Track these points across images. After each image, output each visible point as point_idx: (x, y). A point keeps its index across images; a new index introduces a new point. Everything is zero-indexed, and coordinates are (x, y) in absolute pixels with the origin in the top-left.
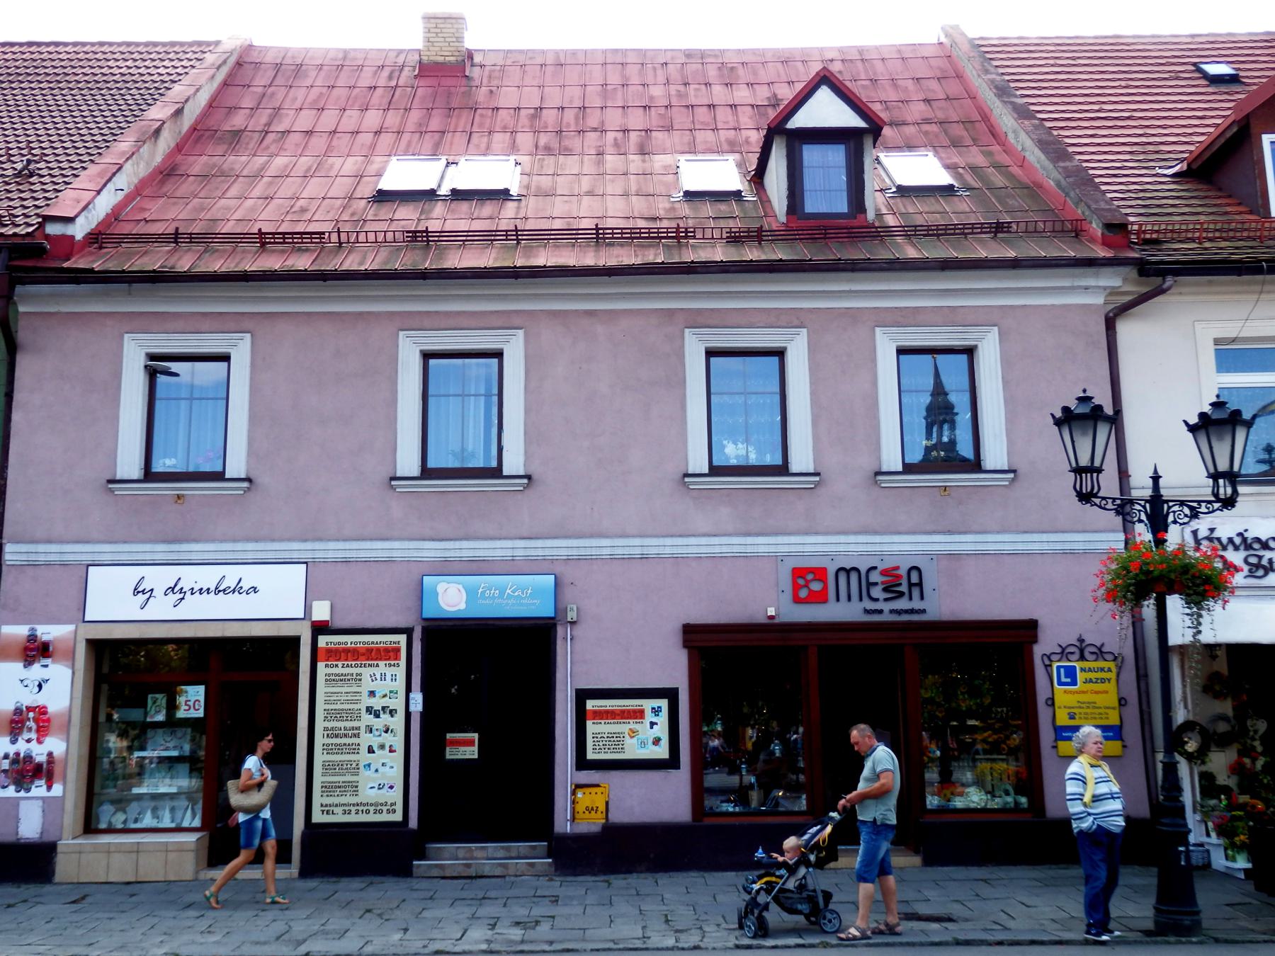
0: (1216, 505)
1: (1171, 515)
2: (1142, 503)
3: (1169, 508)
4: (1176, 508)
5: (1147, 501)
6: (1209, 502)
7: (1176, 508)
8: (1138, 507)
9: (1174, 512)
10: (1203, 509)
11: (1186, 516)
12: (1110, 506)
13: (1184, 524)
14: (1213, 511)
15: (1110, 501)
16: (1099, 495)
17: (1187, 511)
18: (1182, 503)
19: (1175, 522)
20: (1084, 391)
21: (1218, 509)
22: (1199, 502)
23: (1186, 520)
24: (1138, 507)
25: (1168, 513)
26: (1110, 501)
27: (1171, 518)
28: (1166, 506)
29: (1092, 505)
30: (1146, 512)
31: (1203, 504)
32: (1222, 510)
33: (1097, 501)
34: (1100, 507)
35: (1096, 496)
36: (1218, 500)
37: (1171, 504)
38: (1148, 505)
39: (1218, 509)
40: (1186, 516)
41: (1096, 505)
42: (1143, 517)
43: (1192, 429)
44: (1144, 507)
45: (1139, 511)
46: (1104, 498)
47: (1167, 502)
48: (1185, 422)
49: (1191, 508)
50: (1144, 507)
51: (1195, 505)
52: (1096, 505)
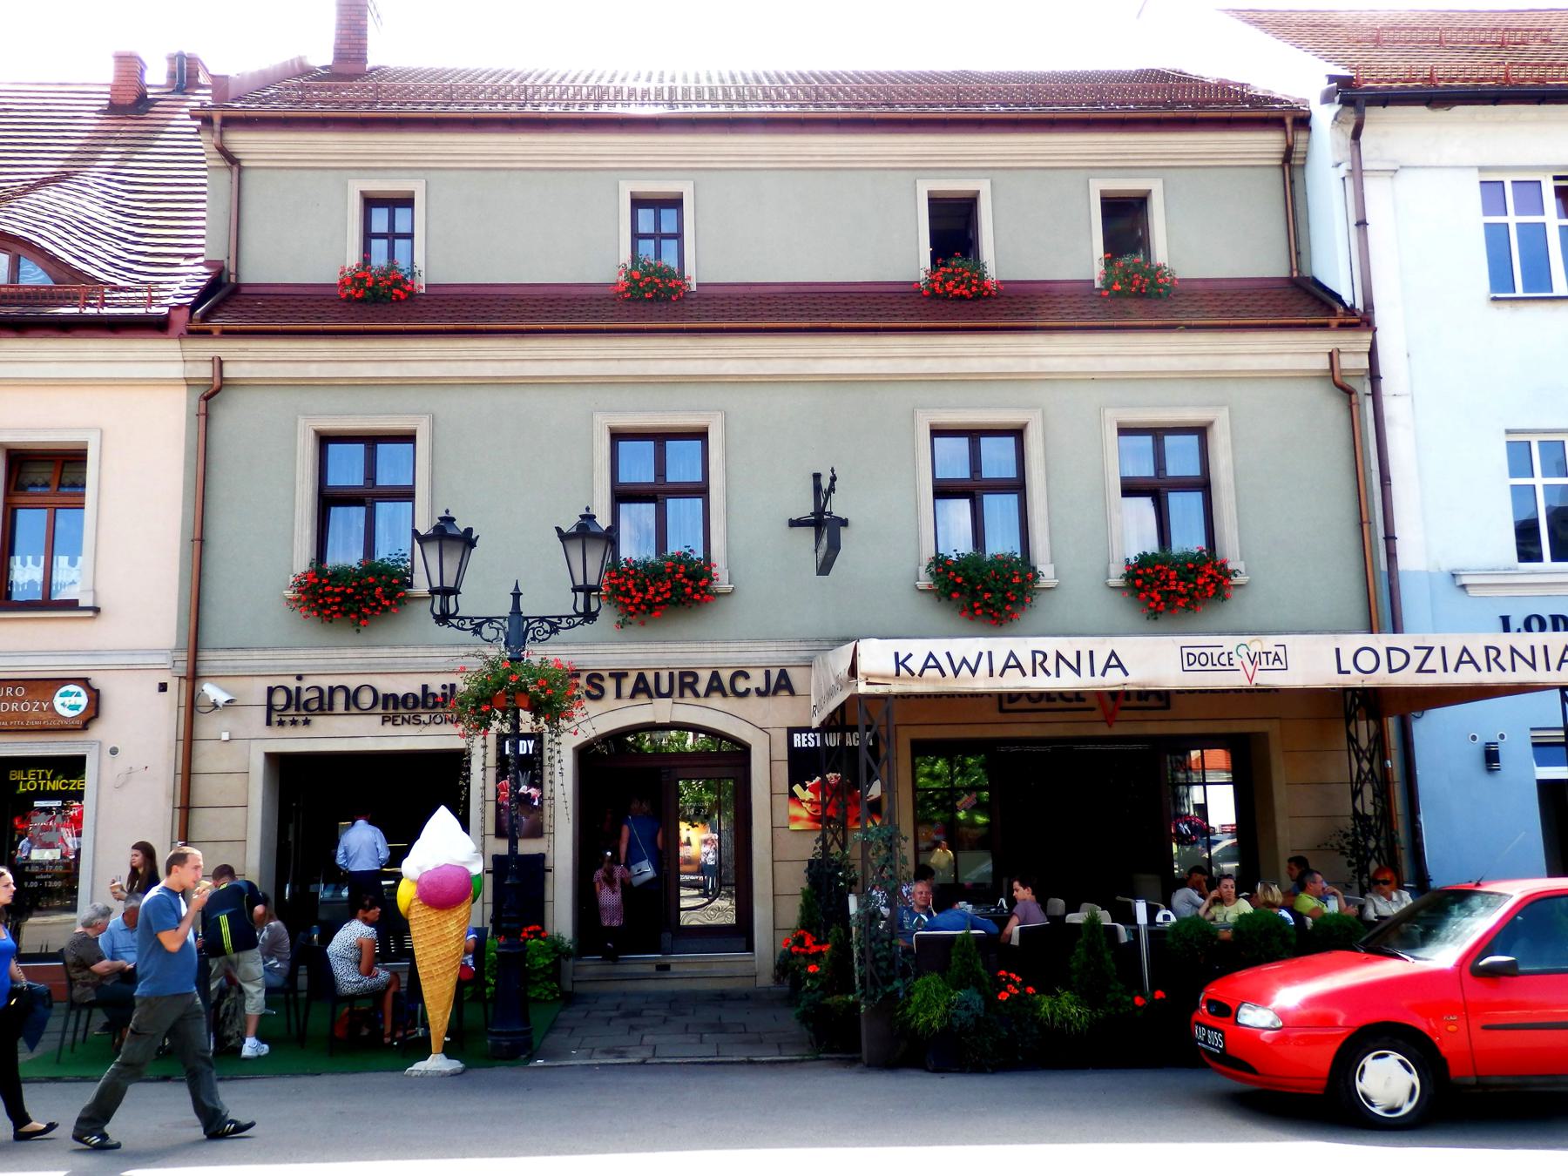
0: (577, 620)
2: (501, 621)
3: (529, 625)
6: (570, 617)
8: (495, 625)
10: (564, 624)
11: (546, 632)
12: (468, 626)
14: (574, 626)
15: (468, 621)
17: (546, 627)
18: (542, 619)
19: (534, 639)
21: (579, 623)
22: (560, 618)
23: (546, 636)
24: (495, 625)
25: (527, 630)
27: (530, 634)
28: (525, 623)
31: (564, 620)
33: (455, 621)
34: (458, 628)
35: (454, 616)
36: (579, 615)
37: (530, 621)
39: (579, 623)
40: (546, 632)
41: (453, 625)
43: (564, 536)
45: (498, 629)
46: (462, 618)
48: (558, 529)
49: (551, 624)
51: (556, 620)
52: (453, 625)
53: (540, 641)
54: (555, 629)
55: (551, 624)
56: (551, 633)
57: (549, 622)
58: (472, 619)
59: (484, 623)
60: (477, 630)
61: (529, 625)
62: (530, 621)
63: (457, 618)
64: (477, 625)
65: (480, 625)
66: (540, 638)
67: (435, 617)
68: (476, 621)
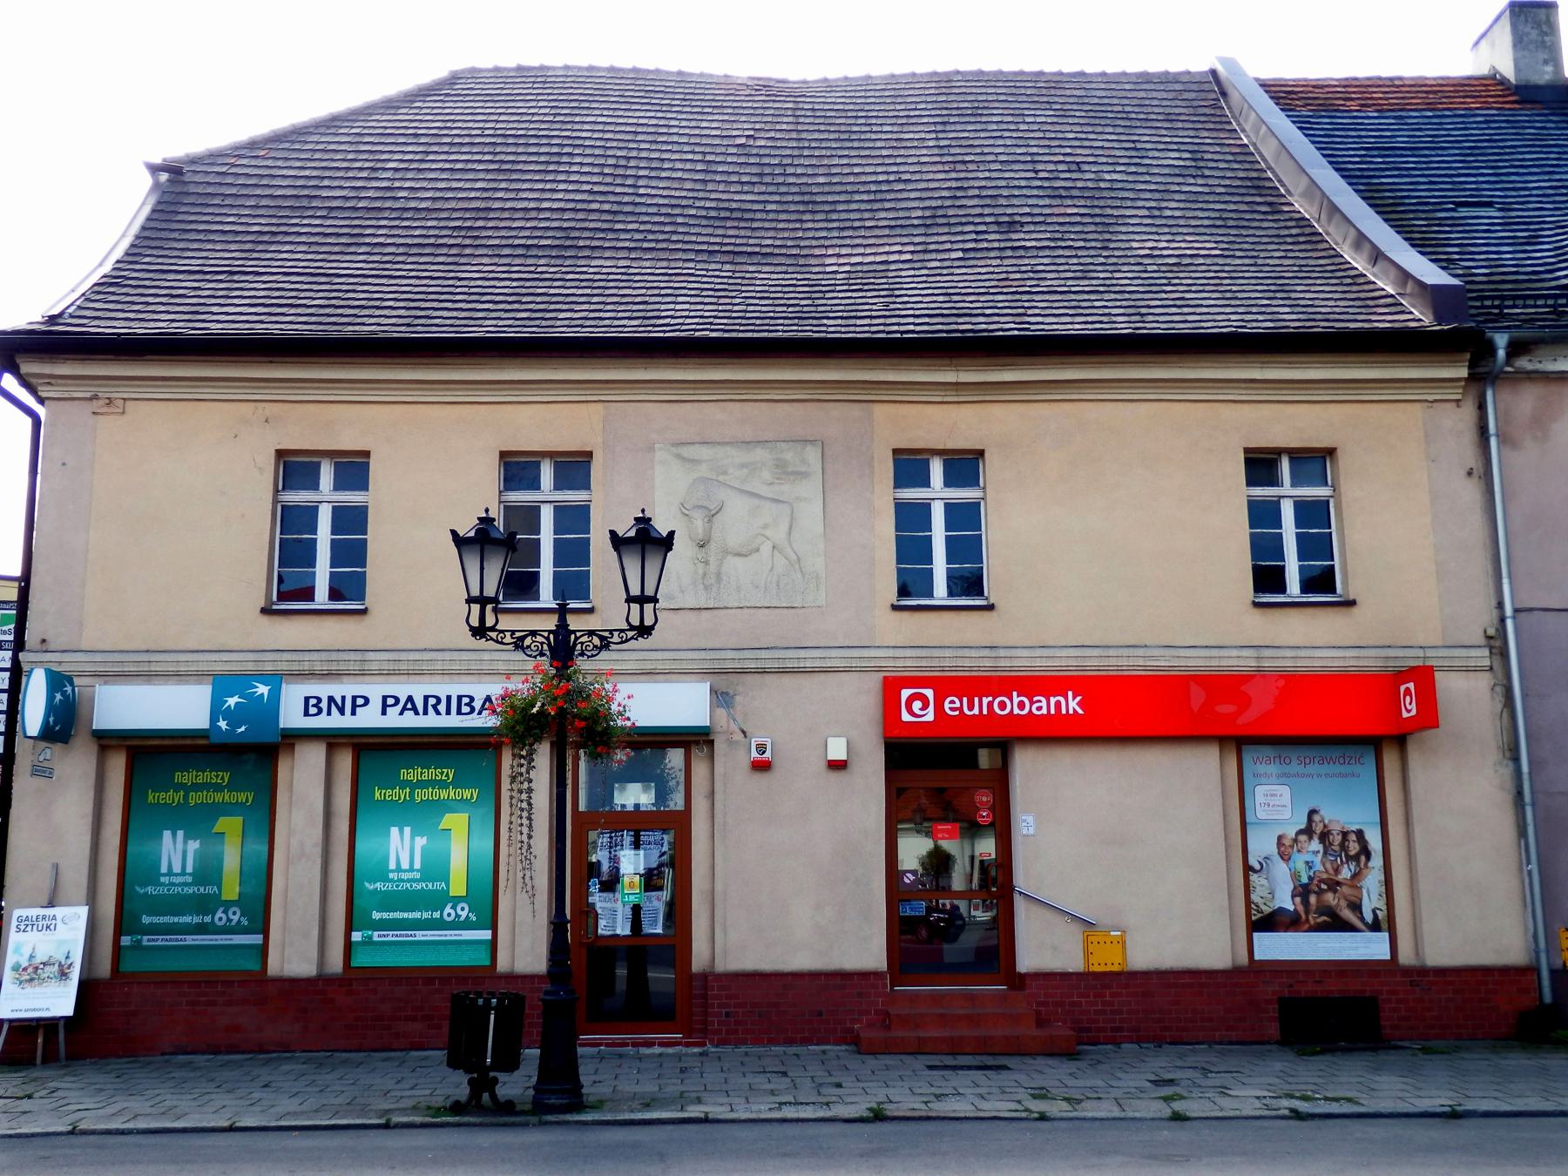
0: (630, 634)
3: (576, 638)
4: (585, 639)
5: (550, 632)
6: (622, 631)
7: (585, 639)
9: (582, 643)
10: (616, 639)
12: (508, 639)
14: (627, 641)
15: (508, 634)
16: (498, 627)
17: (596, 641)
19: (582, 654)
20: (643, 511)
21: (632, 638)
22: (611, 631)
25: (575, 645)
28: (573, 637)
29: (487, 640)
30: (549, 645)
31: (616, 634)
32: (636, 639)
33: (493, 635)
34: (497, 641)
35: (493, 629)
36: (632, 628)
37: (578, 634)
38: (552, 636)
39: (632, 638)
40: (595, 646)
41: (492, 639)
44: (548, 638)
45: (542, 643)
47: (574, 632)
49: (602, 638)
50: (548, 638)
52: (492, 639)
53: (589, 657)
54: (605, 645)
55: (602, 638)
57: (597, 635)
58: (513, 632)
59: (526, 636)
61: (576, 638)
62: (578, 634)
63: (497, 630)
64: (518, 638)
65: (522, 639)
66: (589, 653)
67: (472, 629)
68: (518, 634)
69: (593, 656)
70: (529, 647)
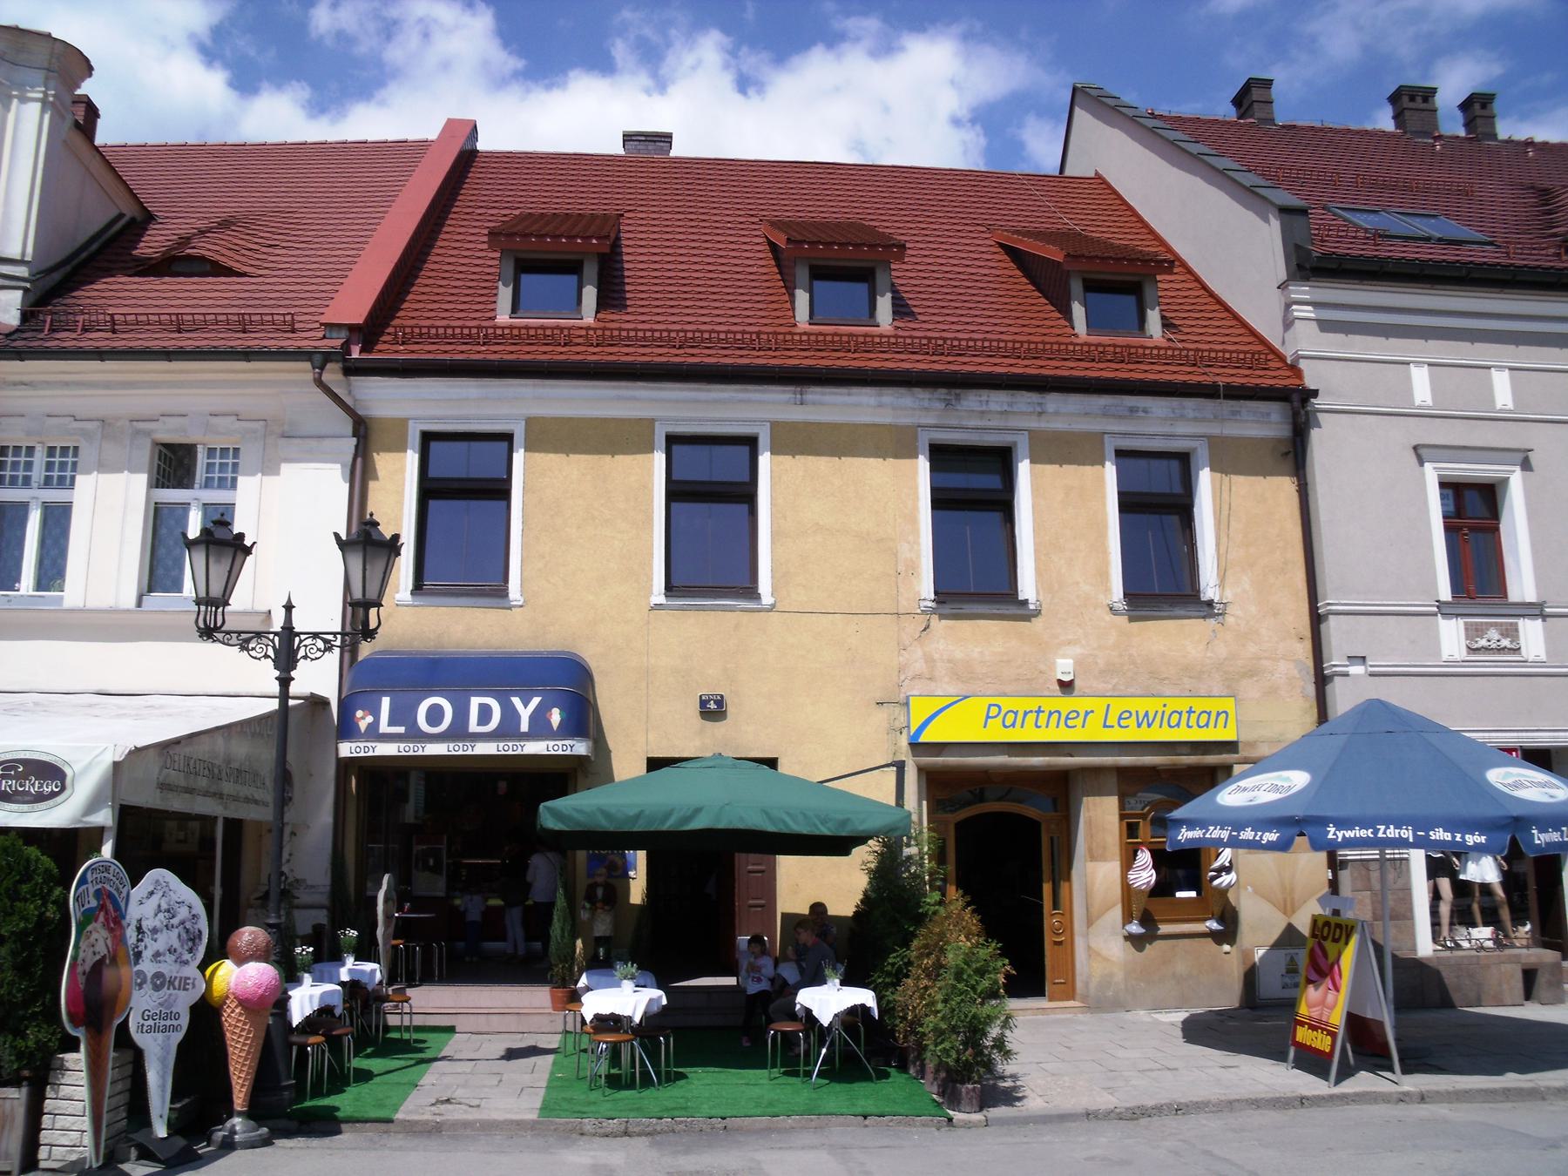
1: (303, 649)
3: (301, 641)
9: (306, 646)
11: (319, 650)
12: (234, 641)
13: (316, 659)
16: (223, 629)
17: (320, 644)
18: (315, 635)
19: (305, 657)
25: (299, 648)
26: (234, 635)
27: (301, 653)
28: (297, 639)
29: (214, 641)
30: (274, 647)
33: (219, 636)
35: (217, 629)
37: (303, 637)
38: (277, 639)
40: (319, 650)
42: (271, 652)
44: (273, 641)
46: (228, 633)
47: (298, 634)
49: (326, 641)
51: (330, 637)
53: (312, 659)
55: (326, 641)
56: (324, 652)
57: (322, 639)
58: (239, 633)
60: (244, 646)
61: (301, 641)
65: (248, 641)
66: (313, 657)
68: (244, 636)
69: (316, 659)
70: (253, 649)
